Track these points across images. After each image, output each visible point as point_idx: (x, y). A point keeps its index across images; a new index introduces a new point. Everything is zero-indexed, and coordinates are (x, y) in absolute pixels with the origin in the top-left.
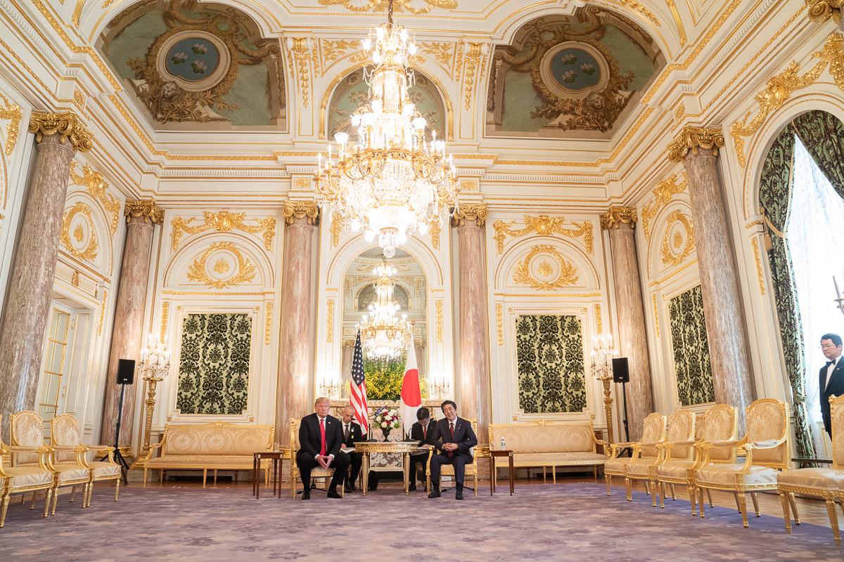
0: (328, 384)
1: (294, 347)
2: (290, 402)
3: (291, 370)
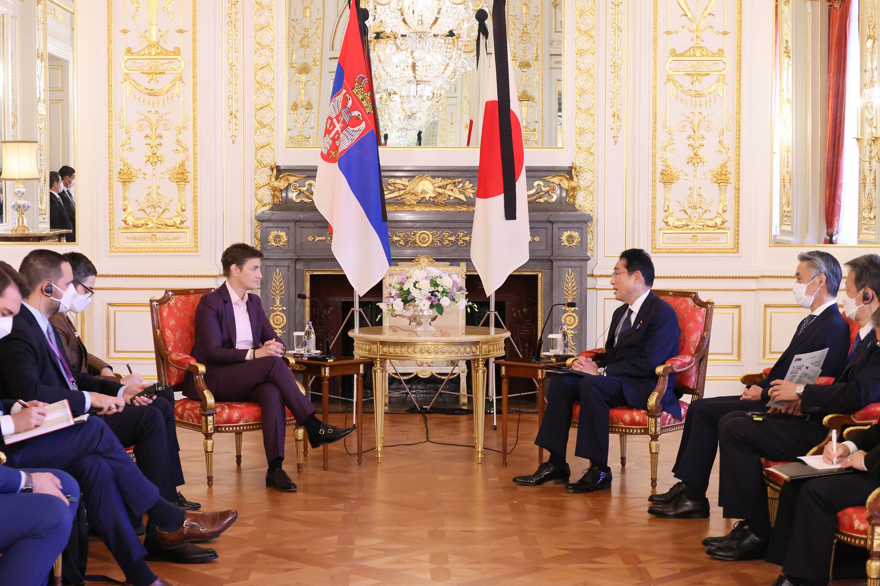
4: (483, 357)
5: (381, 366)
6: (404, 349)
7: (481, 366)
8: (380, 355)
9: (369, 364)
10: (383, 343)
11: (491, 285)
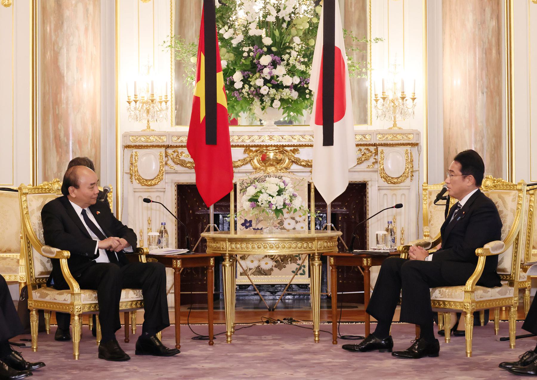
0: (147, 97)
1: (67, 13)
2: (62, 134)
3: (63, 62)
4: (319, 252)
5: (229, 261)
6: (250, 246)
7: (316, 259)
8: (228, 251)
9: (219, 259)
10: (231, 240)
11: (329, 200)
